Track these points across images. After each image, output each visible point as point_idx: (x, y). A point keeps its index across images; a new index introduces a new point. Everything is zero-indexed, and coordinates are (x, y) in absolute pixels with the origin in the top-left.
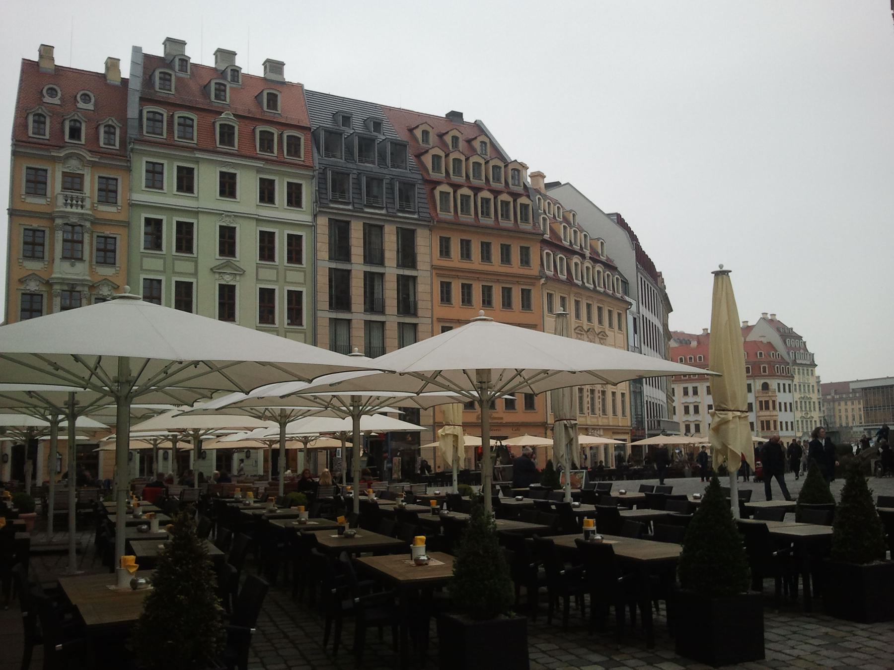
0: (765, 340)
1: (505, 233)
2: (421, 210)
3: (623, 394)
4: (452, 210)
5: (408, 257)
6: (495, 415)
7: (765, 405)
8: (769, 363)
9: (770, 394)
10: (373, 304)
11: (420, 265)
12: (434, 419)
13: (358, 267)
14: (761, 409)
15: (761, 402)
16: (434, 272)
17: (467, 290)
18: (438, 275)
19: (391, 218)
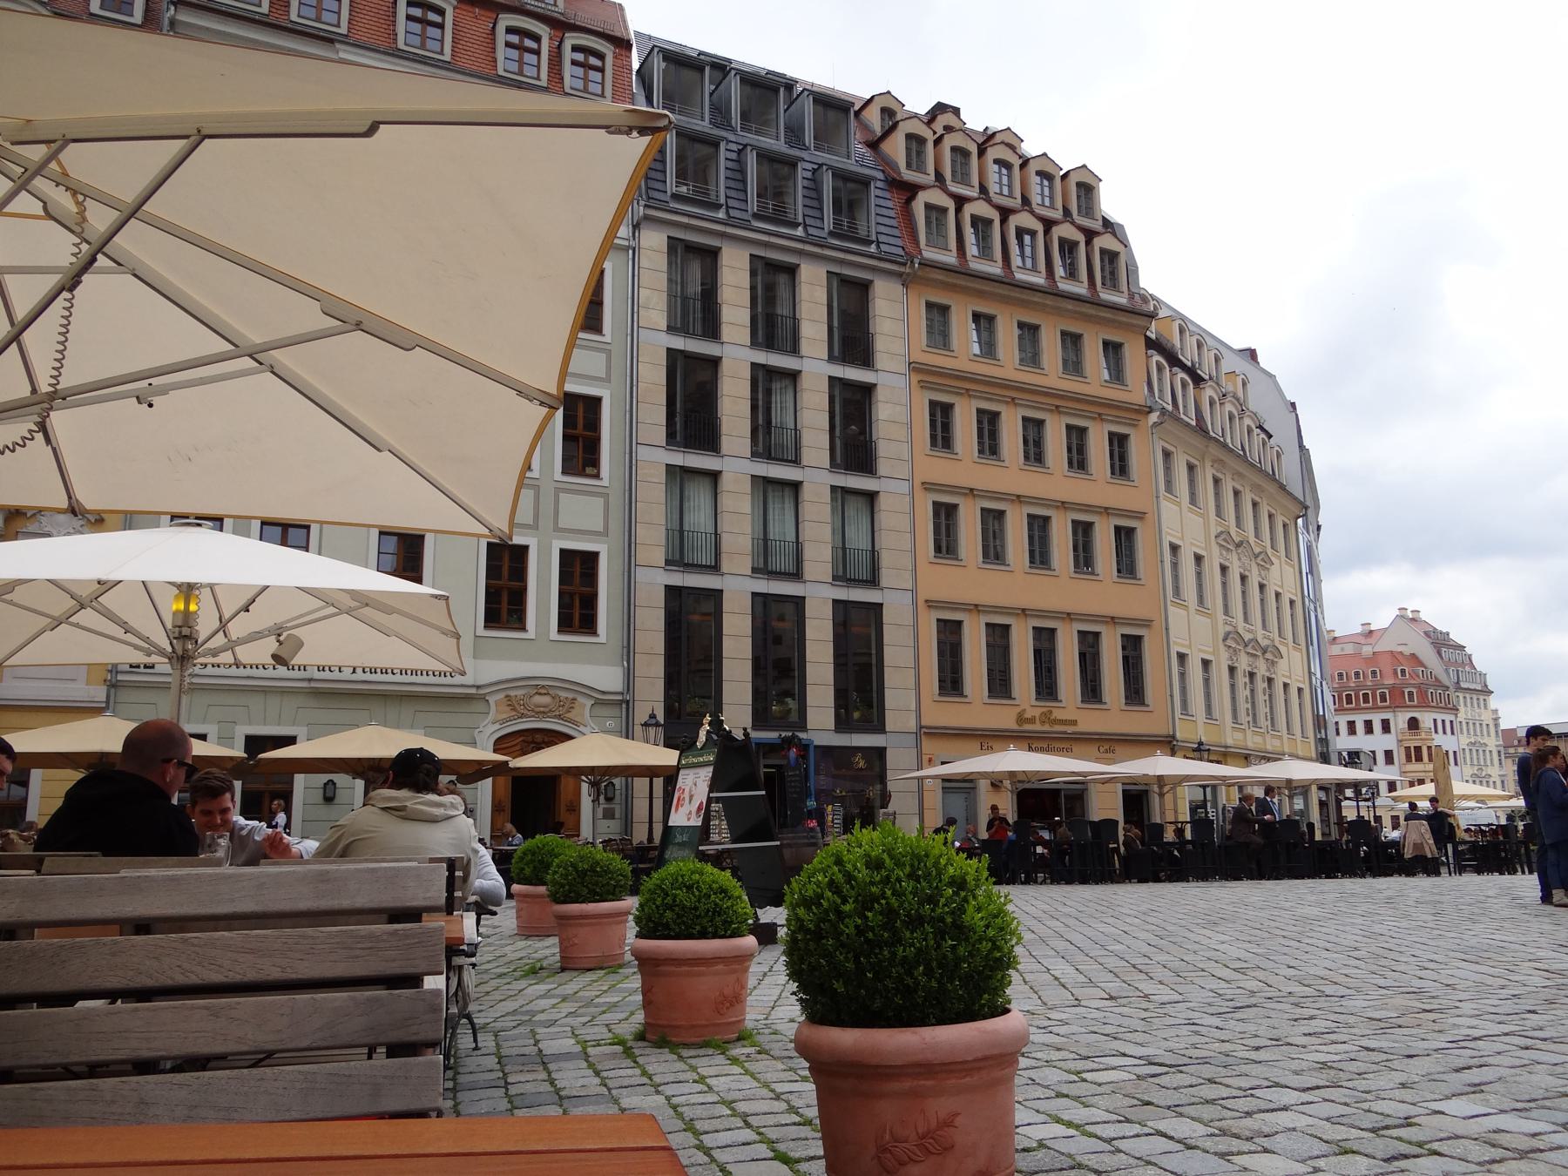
0: (1407, 651)
1: (1069, 305)
2: (882, 238)
3: (1300, 690)
4: (953, 244)
5: (853, 340)
6: (1058, 714)
7: (1415, 754)
8: (1419, 687)
9: (1423, 736)
10: (769, 439)
11: (881, 360)
12: (919, 717)
13: (737, 354)
14: (1409, 759)
15: (1408, 749)
16: (915, 378)
17: (988, 425)
18: (924, 385)
19: (815, 247)
